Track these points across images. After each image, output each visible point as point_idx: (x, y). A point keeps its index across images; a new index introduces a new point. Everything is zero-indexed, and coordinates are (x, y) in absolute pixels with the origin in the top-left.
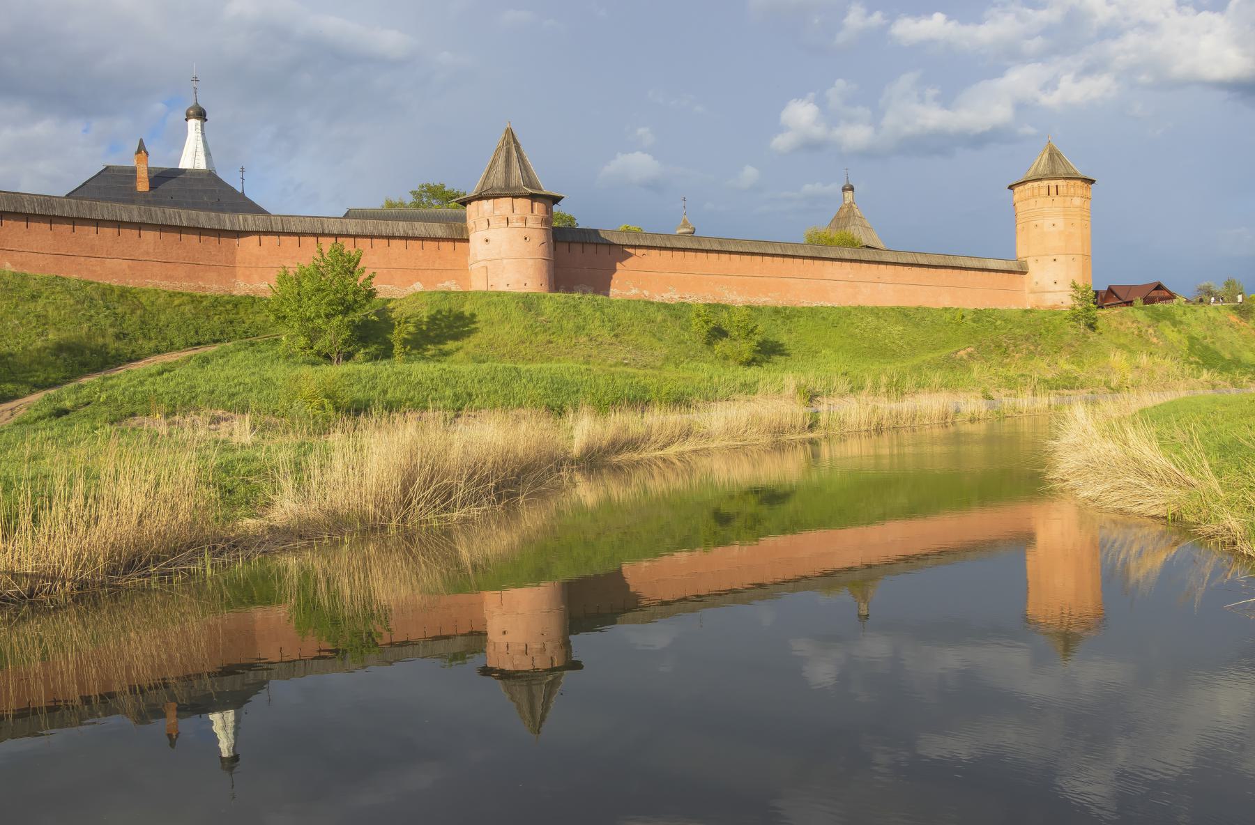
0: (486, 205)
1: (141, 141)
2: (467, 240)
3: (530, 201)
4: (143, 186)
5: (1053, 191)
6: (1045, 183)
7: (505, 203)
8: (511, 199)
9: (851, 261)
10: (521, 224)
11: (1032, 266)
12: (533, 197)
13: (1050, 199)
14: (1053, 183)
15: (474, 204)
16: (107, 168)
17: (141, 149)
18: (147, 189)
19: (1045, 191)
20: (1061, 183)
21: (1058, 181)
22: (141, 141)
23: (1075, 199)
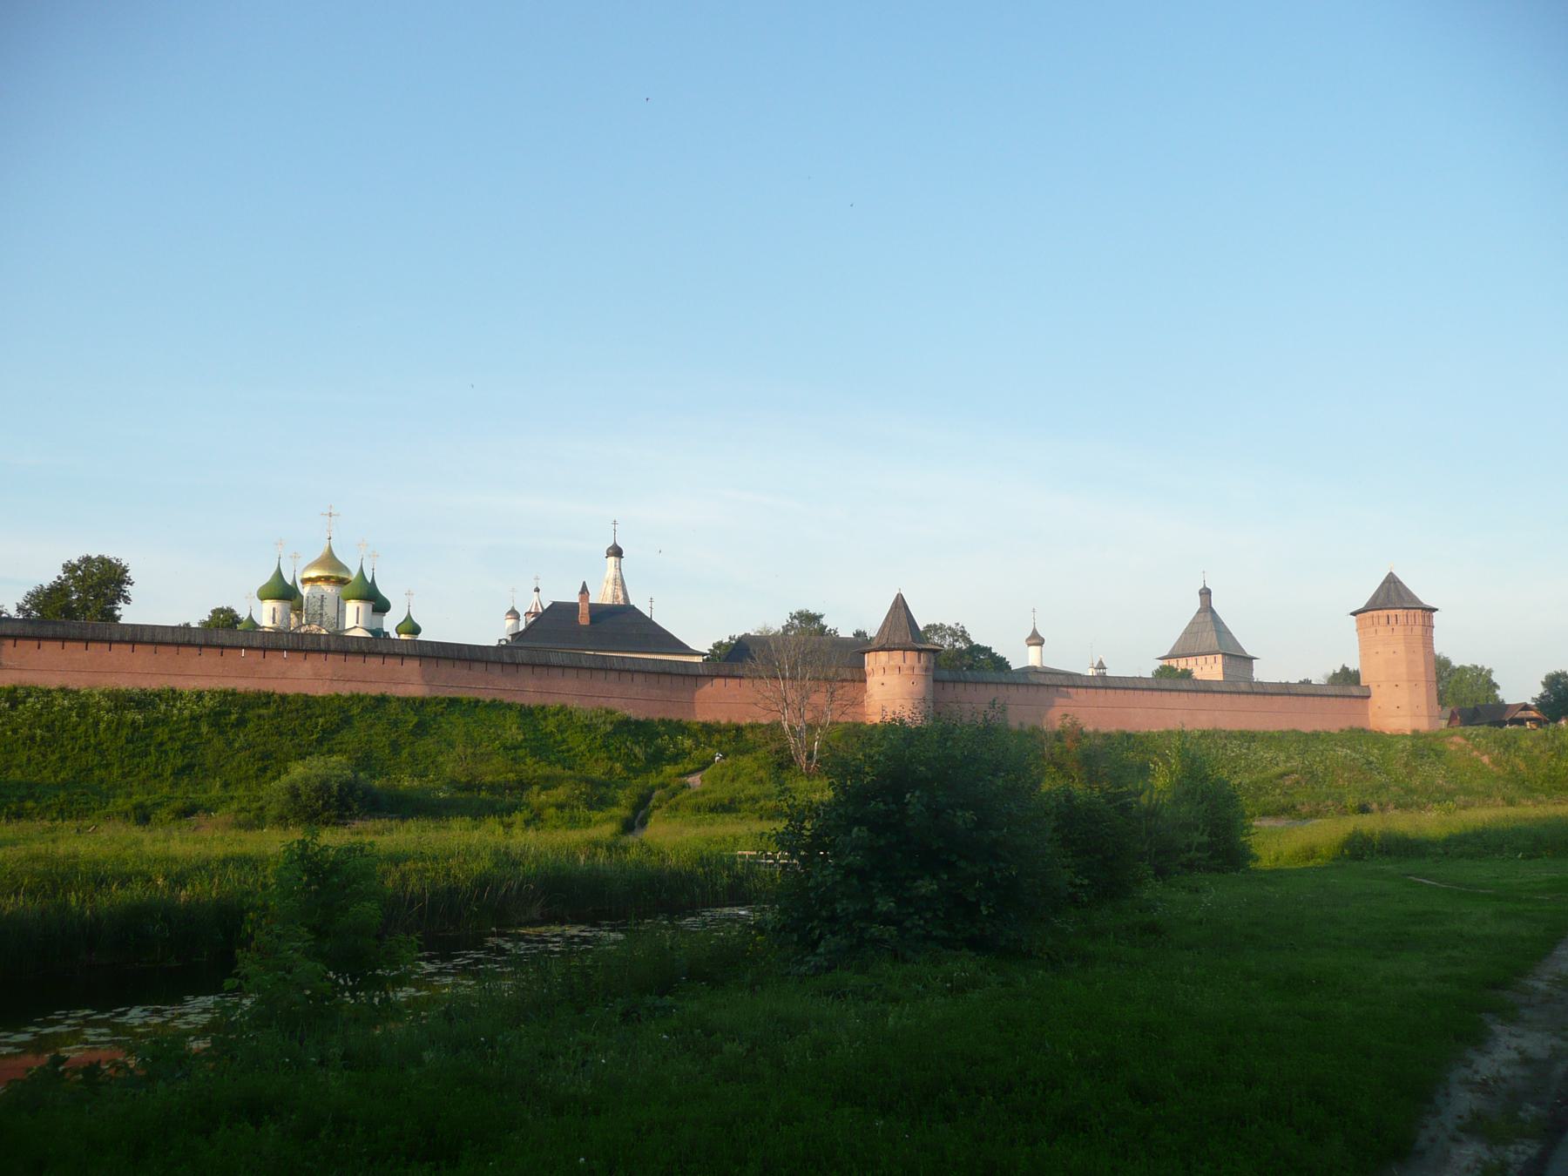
0: (883, 656)
1: (584, 583)
2: (865, 681)
3: (917, 653)
4: (584, 620)
5: (1392, 620)
6: (1386, 612)
7: (898, 655)
8: (902, 652)
9: (1188, 691)
10: (910, 672)
11: (1374, 691)
12: (920, 651)
13: (1389, 628)
14: (1392, 612)
15: (872, 654)
16: (554, 603)
17: (584, 591)
18: (588, 623)
19: (1383, 621)
20: (1399, 612)
21: (1398, 611)
22: (584, 583)
23: (1414, 627)
